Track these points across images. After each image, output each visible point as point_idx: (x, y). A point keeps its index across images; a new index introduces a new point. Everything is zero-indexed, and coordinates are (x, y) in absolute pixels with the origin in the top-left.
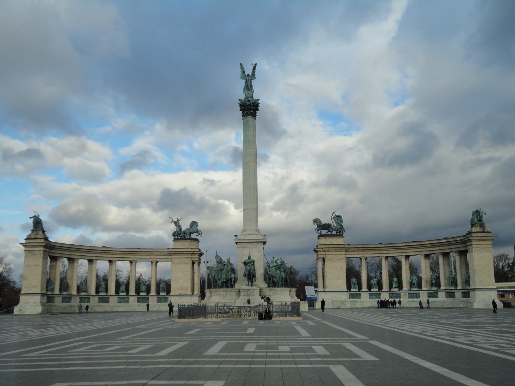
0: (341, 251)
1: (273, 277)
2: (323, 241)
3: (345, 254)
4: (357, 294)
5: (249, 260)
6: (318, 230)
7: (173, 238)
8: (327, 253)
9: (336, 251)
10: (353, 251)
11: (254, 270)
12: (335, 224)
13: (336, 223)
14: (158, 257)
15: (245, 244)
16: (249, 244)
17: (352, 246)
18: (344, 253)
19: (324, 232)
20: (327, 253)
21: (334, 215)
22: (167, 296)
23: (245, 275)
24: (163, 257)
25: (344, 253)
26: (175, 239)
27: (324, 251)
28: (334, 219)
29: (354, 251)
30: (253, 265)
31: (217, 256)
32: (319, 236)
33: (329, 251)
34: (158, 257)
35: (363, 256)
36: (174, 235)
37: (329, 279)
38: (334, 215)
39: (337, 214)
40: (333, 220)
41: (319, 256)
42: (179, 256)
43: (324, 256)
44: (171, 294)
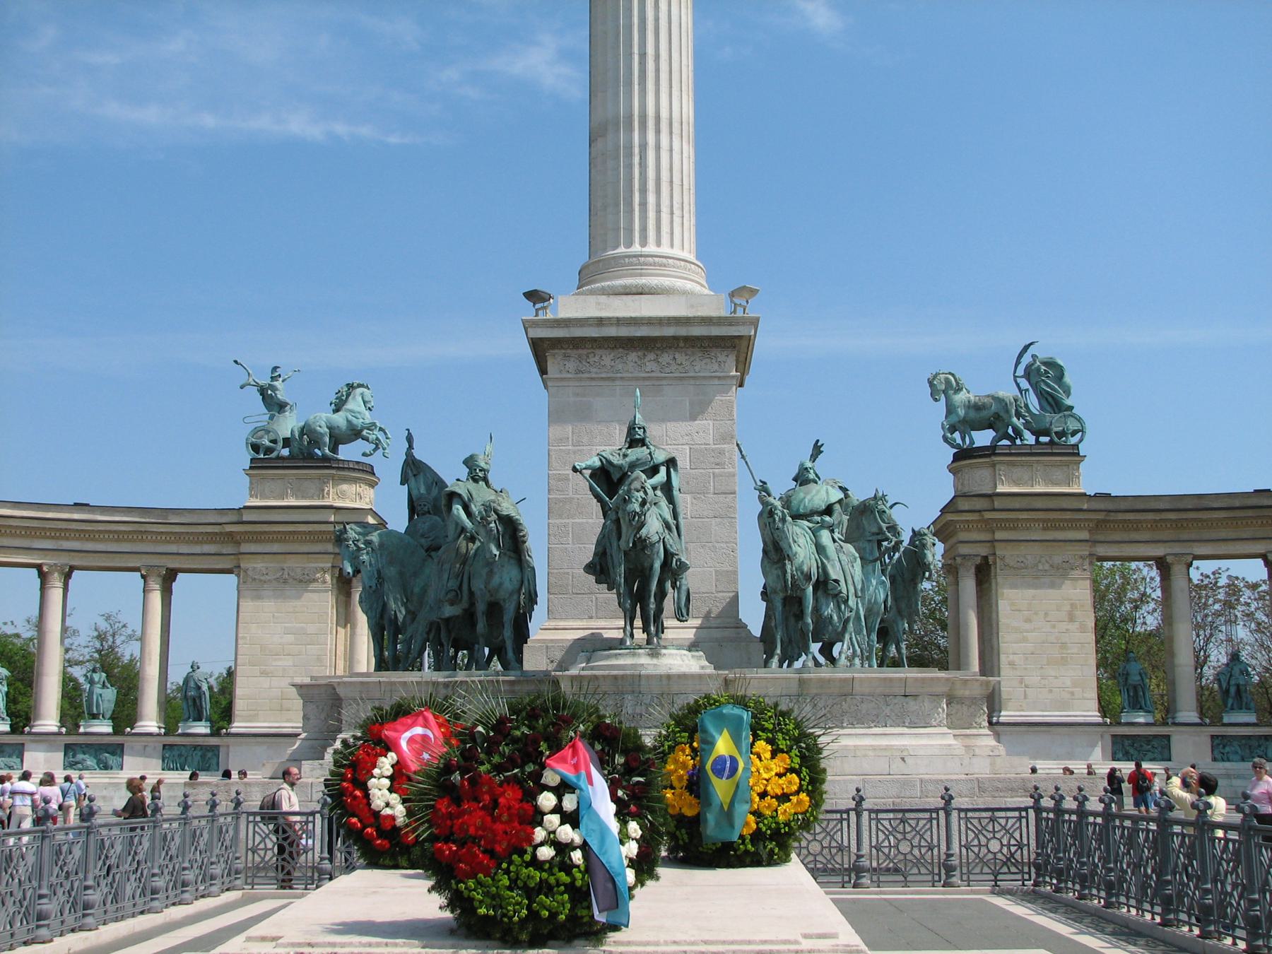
0: (1073, 525)
1: (824, 585)
2: (980, 479)
3: (1095, 542)
4: (1148, 739)
5: (638, 453)
6: (953, 429)
7: (246, 457)
8: (999, 535)
9: (1049, 525)
10: (1127, 526)
11: (673, 526)
12: (1033, 402)
13: (1041, 395)
14: (173, 548)
15: (607, 358)
16: (633, 356)
17: (1123, 506)
18: (1084, 535)
19: (983, 438)
20: (999, 535)
21: (1027, 359)
22: (214, 741)
23: (600, 568)
24: (197, 549)
25: (1084, 535)
26: (255, 465)
27: (990, 526)
28: (1028, 374)
29: (1136, 526)
30: (667, 488)
31: (413, 469)
32: (956, 458)
33: (1013, 525)
34: (173, 548)
35: (1177, 549)
36: (256, 447)
37: (1011, 664)
38: (1027, 359)
39: (1041, 352)
40: (1024, 384)
41: (964, 549)
42: (276, 548)
43: (983, 551)
44: (238, 726)
